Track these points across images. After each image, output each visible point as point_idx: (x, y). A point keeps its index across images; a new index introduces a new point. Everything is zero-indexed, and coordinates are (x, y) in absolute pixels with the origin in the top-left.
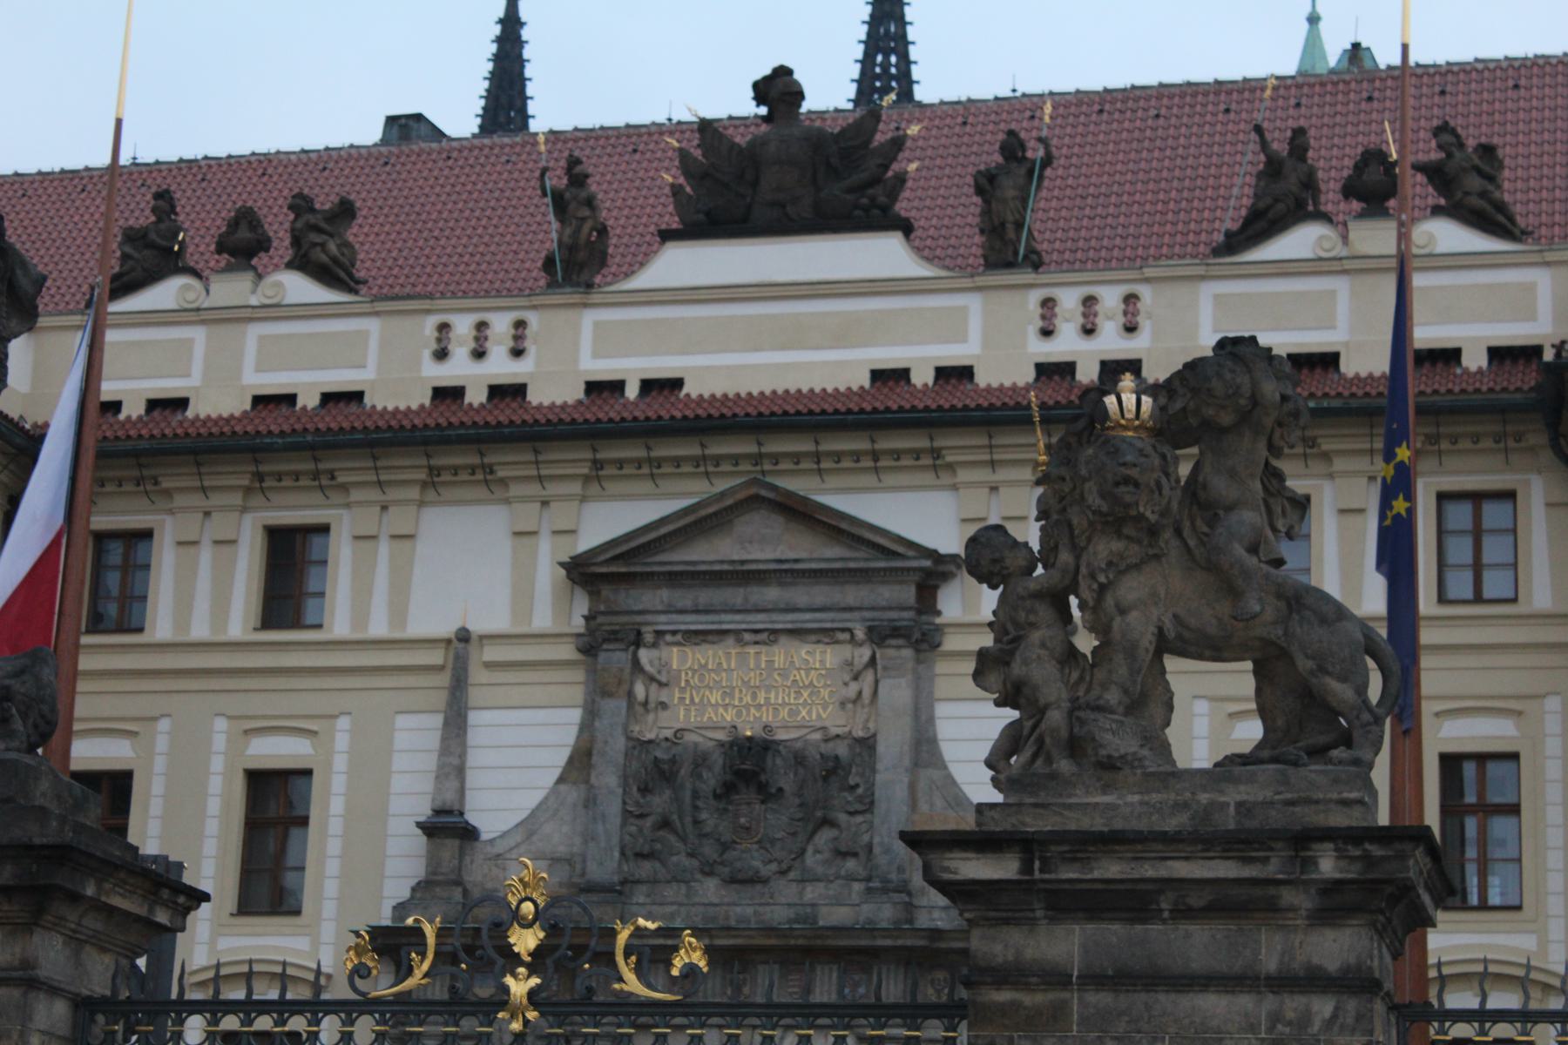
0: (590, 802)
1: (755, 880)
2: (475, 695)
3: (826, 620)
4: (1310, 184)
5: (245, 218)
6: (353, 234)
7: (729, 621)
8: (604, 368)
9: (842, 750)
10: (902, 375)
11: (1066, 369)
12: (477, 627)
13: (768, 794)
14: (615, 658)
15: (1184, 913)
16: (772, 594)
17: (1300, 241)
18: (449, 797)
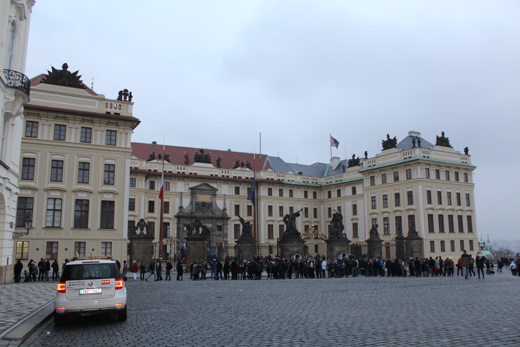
0: (192, 206)
1: (205, 212)
2: (183, 197)
3: (208, 193)
4: (239, 164)
5: (160, 155)
6: (169, 157)
7: (202, 193)
8: (191, 172)
9: (210, 203)
10: (213, 175)
11: (224, 176)
12: (183, 192)
13: (205, 206)
14: (194, 195)
16: (205, 191)
17: (239, 168)
18: (181, 205)
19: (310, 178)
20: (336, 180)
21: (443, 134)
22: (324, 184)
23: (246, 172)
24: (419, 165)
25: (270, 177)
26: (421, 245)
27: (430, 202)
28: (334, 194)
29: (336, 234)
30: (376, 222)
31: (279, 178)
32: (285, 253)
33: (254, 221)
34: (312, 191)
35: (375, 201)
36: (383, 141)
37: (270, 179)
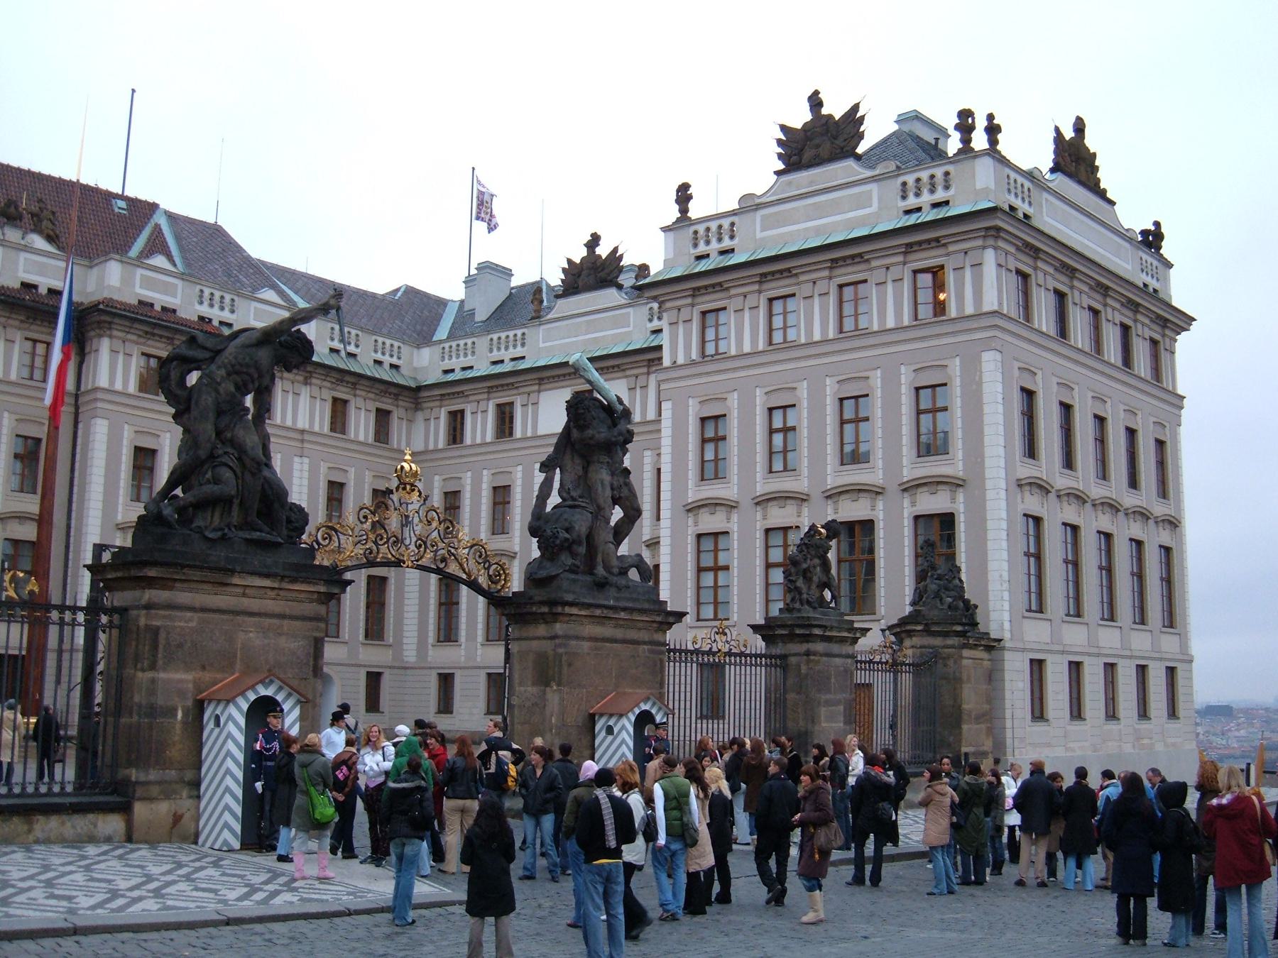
15: (836, 642)
19: (367, 341)
20: (496, 355)
21: (1079, 127)
22: (434, 377)
23: (23, 256)
24: (991, 242)
25: (160, 299)
26: (993, 676)
27: (1031, 451)
28: (480, 426)
29: (582, 550)
30: (721, 555)
31: (205, 310)
32: (150, 675)
33: (44, 520)
34: (372, 406)
35: (719, 439)
36: (784, 128)
37: (158, 308)
